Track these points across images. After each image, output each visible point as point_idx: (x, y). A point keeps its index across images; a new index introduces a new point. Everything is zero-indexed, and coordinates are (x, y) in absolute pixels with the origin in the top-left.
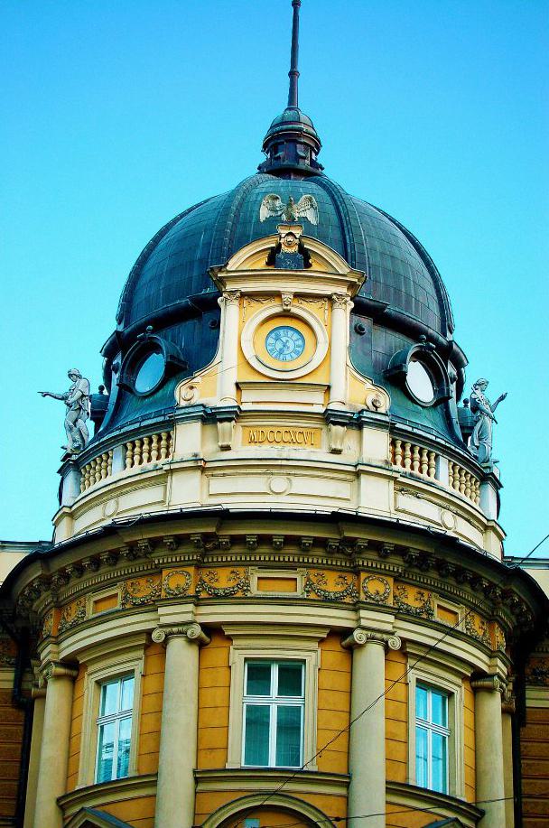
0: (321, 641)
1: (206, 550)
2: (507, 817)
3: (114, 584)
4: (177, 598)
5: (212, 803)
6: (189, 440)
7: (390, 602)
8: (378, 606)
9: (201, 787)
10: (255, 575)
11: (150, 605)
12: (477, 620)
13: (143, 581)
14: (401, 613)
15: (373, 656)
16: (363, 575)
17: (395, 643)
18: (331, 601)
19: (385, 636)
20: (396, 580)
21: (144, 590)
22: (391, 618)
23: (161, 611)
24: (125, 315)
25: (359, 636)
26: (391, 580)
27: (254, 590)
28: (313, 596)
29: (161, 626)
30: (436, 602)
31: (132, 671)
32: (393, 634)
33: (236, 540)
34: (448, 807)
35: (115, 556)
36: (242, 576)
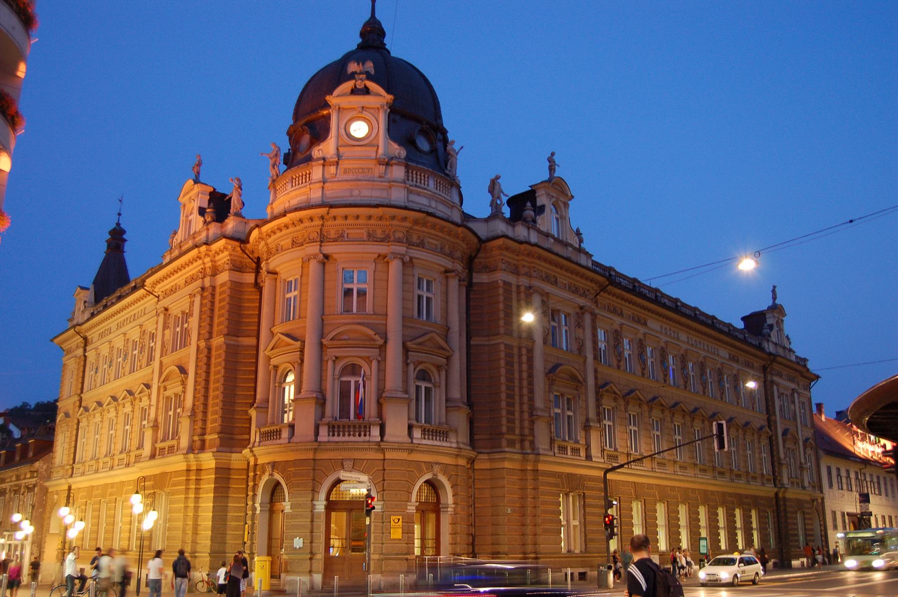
6: (317, 172)
17: (407, 259)
24: (297, 115)
33: (335, 218)
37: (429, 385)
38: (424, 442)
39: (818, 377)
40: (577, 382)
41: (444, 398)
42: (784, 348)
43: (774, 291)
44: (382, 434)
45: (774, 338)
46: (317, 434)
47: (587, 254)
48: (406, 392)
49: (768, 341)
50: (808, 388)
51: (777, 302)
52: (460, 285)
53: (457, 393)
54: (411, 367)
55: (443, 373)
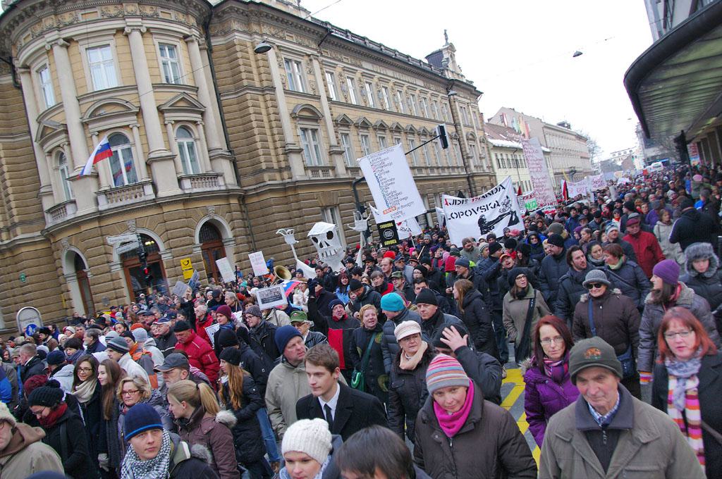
0: (114, 35)
1: (56, 7)
2: (209, 89)
3: (27, 30)
4: (50, 29)
5: (85, 107)
7: (138, 13)
8: (133, 16)
9: (81, 102)
10: (80, 13)
11: (41, 35)
12: (181, 15)
13: (37, 26)
14: (144, 17)
15: (136, 36)
16: (124, 4)
17: (144, 30)
18: (113, 17)
19: (139, 28)
20: (139, 4)
21: (38, 29)
22: (140, 20)
23: (46, 36)
25: (127, 30)
26: (137, 4)
27: (81, 19)
28: (105, 17)
29: (48, 43)
30: (159, 11)
31: (45, 64)
32: (142, 26)
34: (181, 88)
35: (22, 18)
36: (74, 14)
37: (190, 140)
38: (195, 190)
39: (482, 93)
40: (315, 117)
41: (206, 148)
42: (458, 74)
43: (445, 34)
44: (156, 191)
45: (451, 67)
46: (97, 204)
47: (305, 10)
48: (170, 150)
49: (447, 70)
50: (476, 102)
51: (449, 41)
52: (200, 49)
53: (218, 142)
54: (170, 126)
55: (201, 127)
